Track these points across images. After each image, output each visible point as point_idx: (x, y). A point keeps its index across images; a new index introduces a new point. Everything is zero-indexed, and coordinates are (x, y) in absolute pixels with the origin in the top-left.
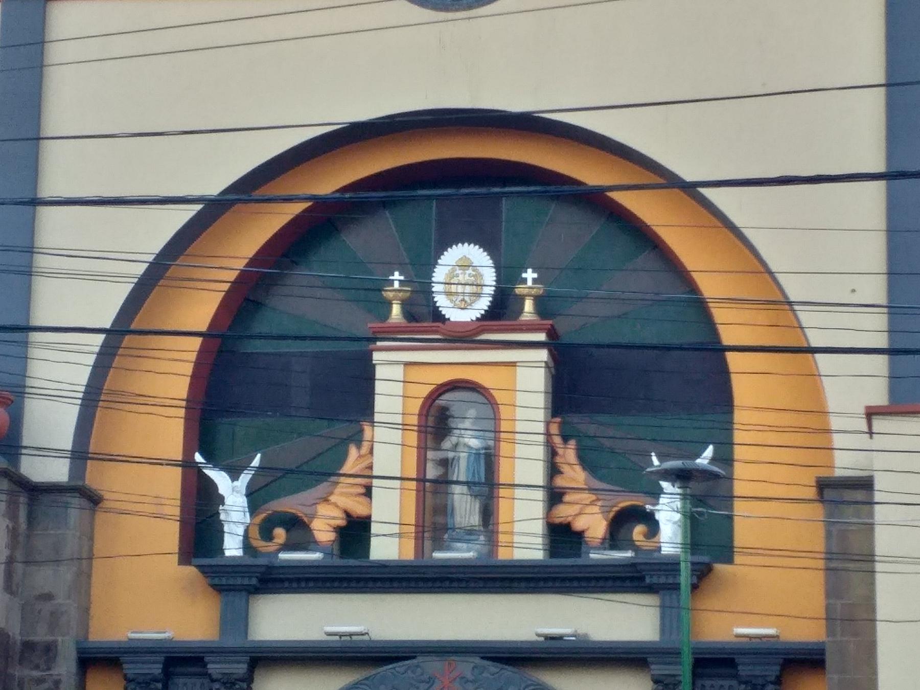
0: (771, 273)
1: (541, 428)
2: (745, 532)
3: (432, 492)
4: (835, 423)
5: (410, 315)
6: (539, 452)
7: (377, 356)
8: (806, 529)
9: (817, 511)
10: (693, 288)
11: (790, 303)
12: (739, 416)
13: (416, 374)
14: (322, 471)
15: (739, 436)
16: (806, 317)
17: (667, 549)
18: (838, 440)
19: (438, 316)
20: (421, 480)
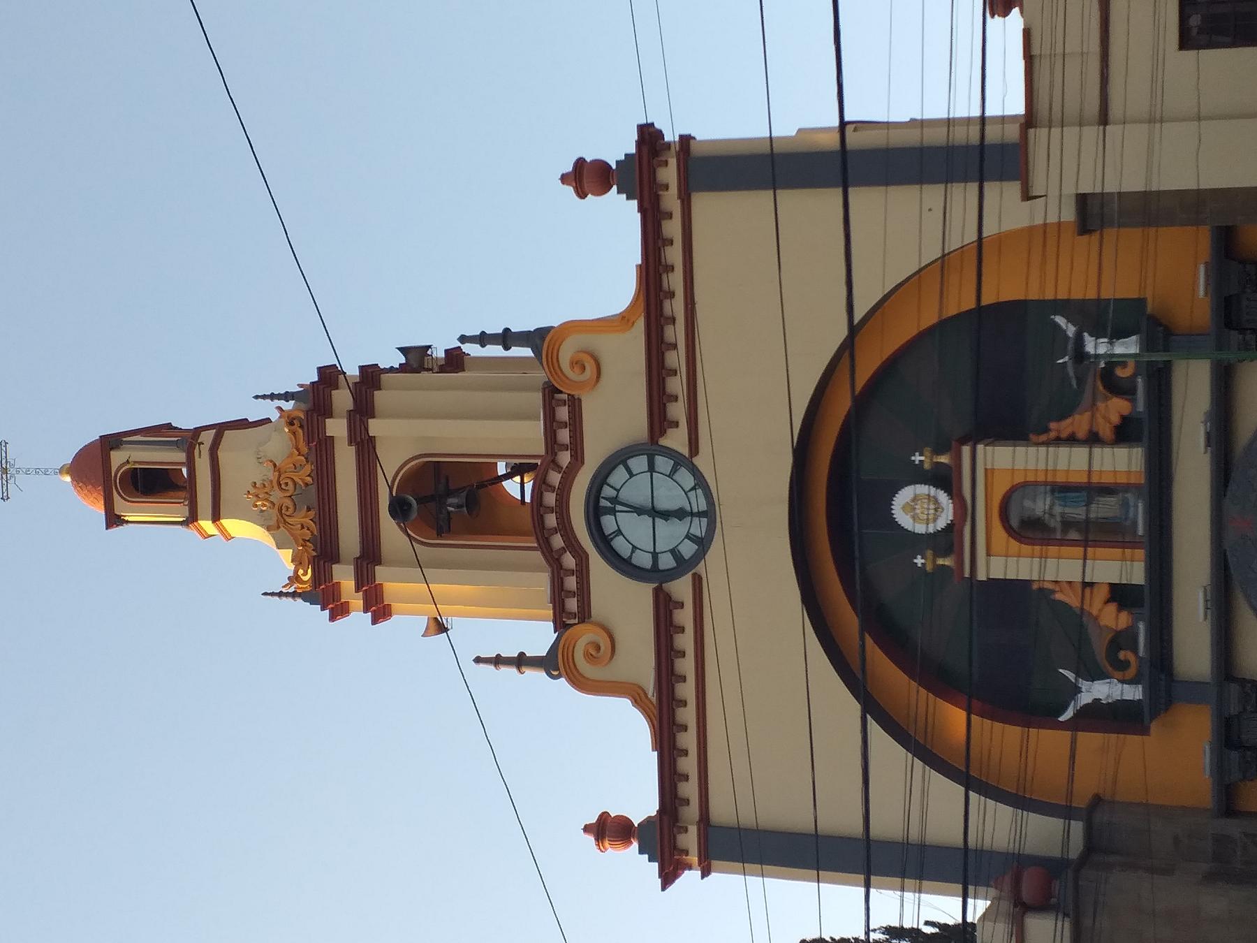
0: (920, 270)
1: (1043, 449)
2: (1128, 290)
3: (1093, 535)
4: (1039, 221)
5: (946, 553)
6: (1063, 451)
7: (981, 576)
8: (1125, 243)
9: (1110, 233)
10: (931, 330)
11: (944, 256)
12: (1034, 295)
14: (1074, 623)
15: (1049, 295)
16: (954, 244)
18: (1052, 219)
19: (950, 528)
20: (1085, 543)
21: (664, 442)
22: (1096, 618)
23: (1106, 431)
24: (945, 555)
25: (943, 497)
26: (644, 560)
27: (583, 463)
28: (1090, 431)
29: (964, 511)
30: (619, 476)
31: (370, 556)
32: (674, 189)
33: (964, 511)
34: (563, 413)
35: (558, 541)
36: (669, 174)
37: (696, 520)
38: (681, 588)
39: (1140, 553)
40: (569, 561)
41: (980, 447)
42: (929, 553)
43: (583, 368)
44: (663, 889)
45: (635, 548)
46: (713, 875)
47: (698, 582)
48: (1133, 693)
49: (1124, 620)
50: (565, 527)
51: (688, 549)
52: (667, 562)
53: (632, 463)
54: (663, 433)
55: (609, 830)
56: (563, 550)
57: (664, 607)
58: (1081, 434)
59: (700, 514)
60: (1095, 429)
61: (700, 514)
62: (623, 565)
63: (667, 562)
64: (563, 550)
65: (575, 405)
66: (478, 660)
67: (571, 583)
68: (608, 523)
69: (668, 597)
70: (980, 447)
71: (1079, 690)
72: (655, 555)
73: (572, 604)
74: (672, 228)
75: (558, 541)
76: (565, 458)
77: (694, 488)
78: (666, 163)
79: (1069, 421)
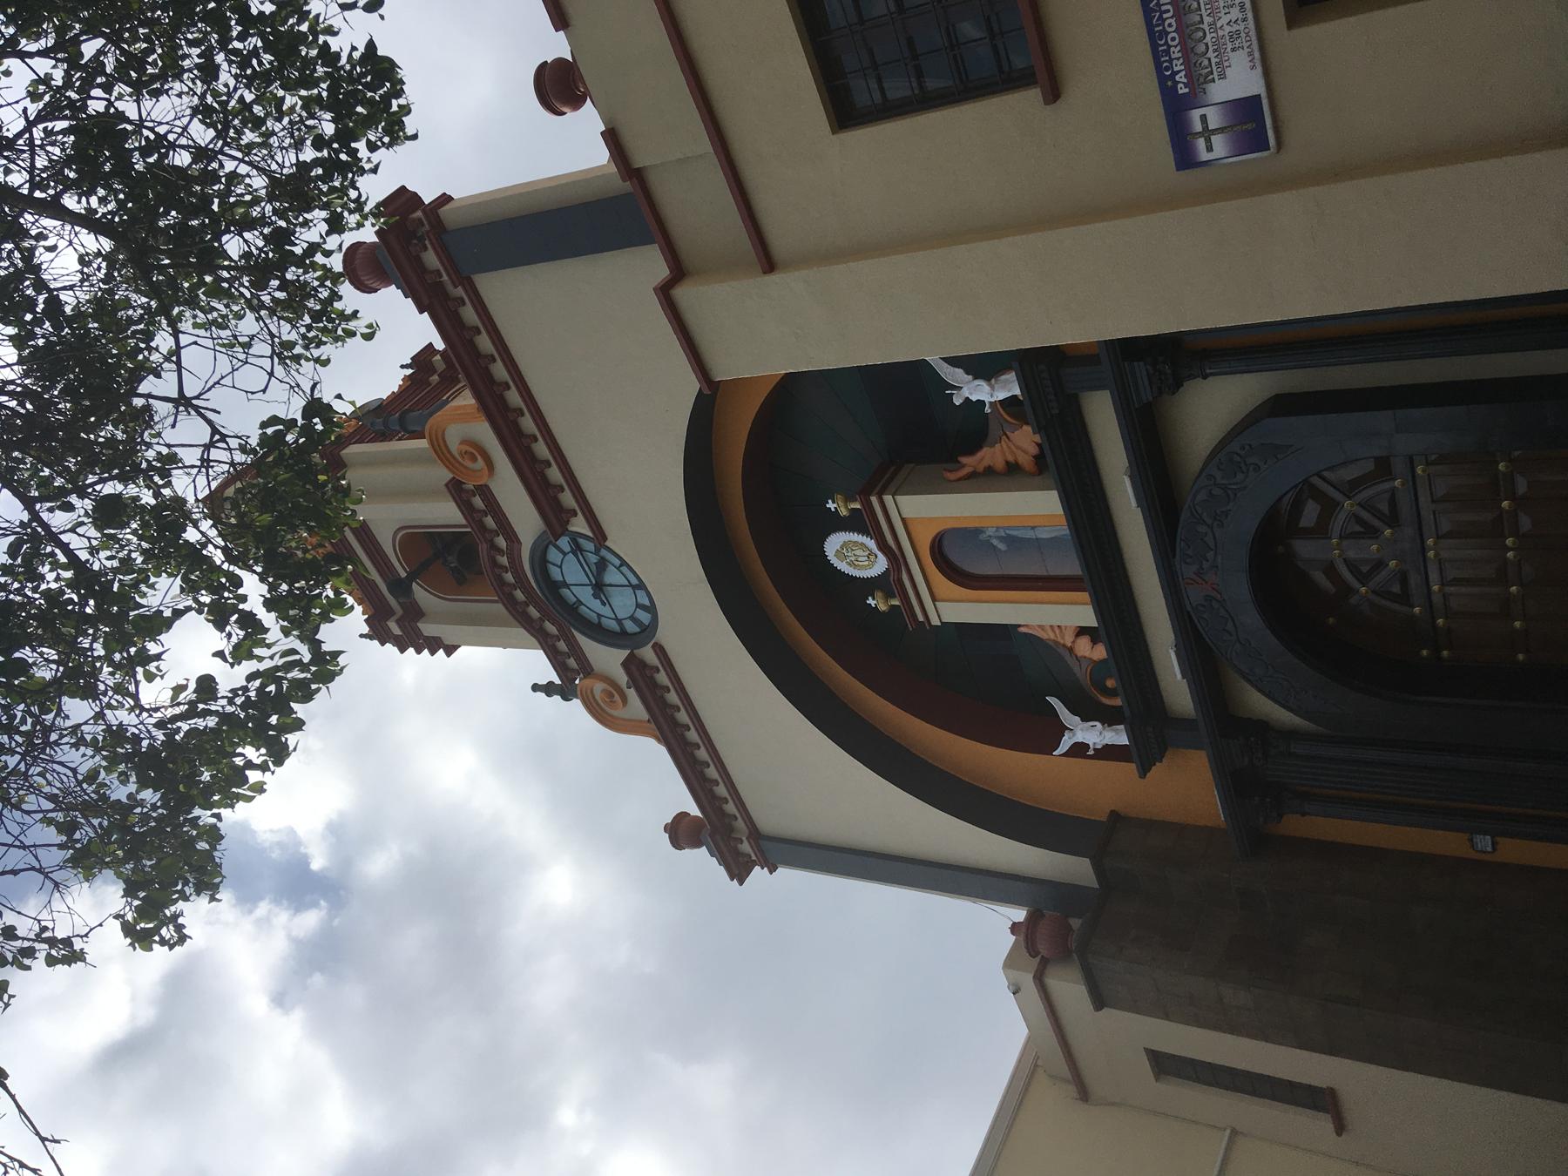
13: (938, 592)
17: (1017, 391)
21: (572, 528)
22: (1071, 650)
23: (1025, 461)
24: (893, 596)
25: (871, 544)
26: (613, 625)
27: (520, 543)
28: (1007, 462)
29: (896, 558)
30: (553, 555)
31: (413, 614)
32: (445, 277)
33: (896, 558)
34: (478, 502)
35: (533, 612)
36: (431, 259)
37: (640, 593)
38: (648, 654)
40: (551, 628)
41: (888, 499)
42: (879, 594)
43: (474, 459)
44: (741, 883)
45: (599, 616)
46: (779, 870)
47: (660, 650)
48: (1118, 736)
49: (1100, 652)
51: (644, 617)
55: (681, 832)
56: (541, 620)
58: (999, 464)
60: (1011, 458)
62: (598, 631)
63: (631, 627)
64: (541, 620)
65: (485, 492)
66: (536, 688)
67: (562, 646)
68: (565, 592)
69: (643, 665)
70: (888, 499)
71: (1062, 729)
72: (619, 621)
73: (572, 662)
74: (469, 314)
75: (533, 612)
76: (501, 542)
78: (426, 249)
79: (979, 455)
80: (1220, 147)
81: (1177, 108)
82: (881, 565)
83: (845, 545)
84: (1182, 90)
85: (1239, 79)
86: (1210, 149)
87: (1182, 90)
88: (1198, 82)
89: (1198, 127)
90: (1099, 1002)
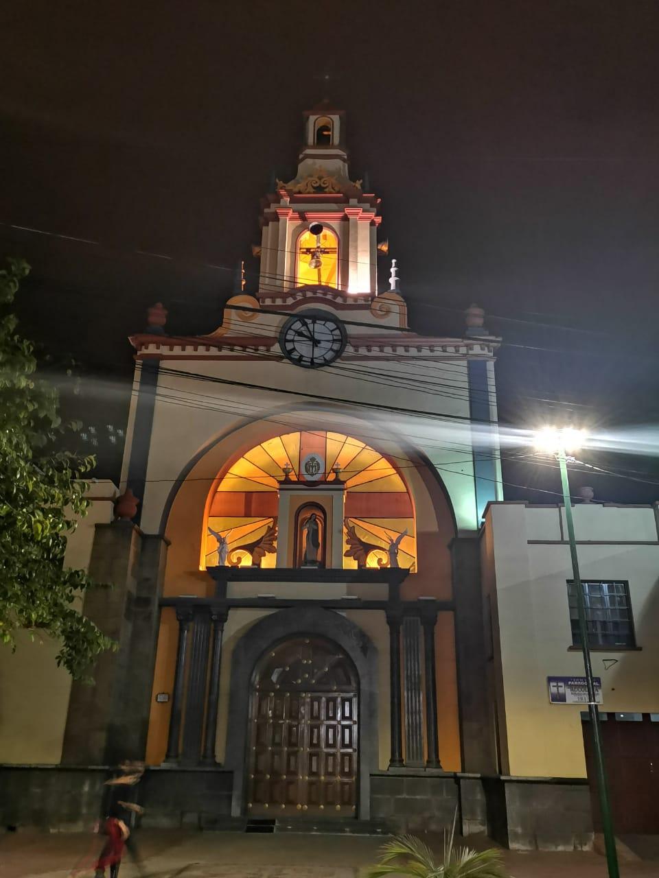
30: (331, 325)
38: (276, 349)
39: (291, 567)
40: (290, 301)
47: (278, 358)
50: (306, 300)
51: (295, 355)
52: (289, 346)
53: (337, 332)
54: (354, 346)
56: (295, 299)
57: (267, 342)
59: (312, 362)
61: (312, 362)
68: (309, 321)
72: (293, 341)
77: (325, 359)
80: (554, 690)
81: (566, 680)
82: (309, 478)
83: (318, 464)
84: (569, 683)
85: (571, 698)
86: (553, 686)
87: (569, 683)
88: (571, 687)
89: (559, 684)
90: (99, 527)
